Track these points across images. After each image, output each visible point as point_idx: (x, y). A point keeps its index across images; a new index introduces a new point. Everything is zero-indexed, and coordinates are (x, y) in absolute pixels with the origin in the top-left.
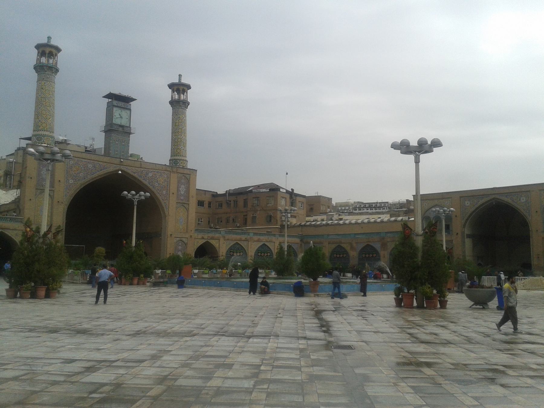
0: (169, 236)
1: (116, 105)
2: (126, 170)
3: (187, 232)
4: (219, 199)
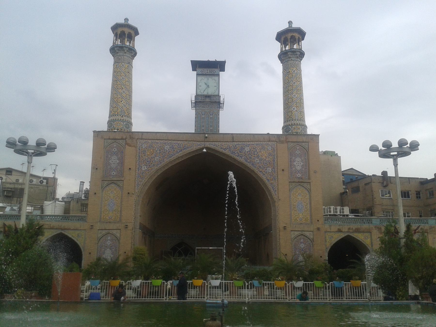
1: (201, 73)
2: (212, 146)
3: (312, 223)
4: (429, 186)
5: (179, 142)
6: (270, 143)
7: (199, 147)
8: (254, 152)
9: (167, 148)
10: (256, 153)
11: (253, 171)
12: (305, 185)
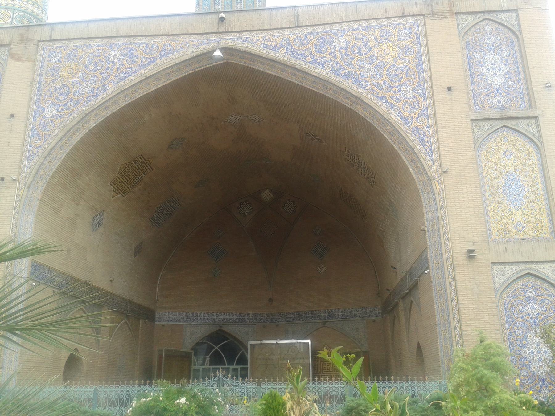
0: (460, 258)
5: (148, 40)
6: (403, 21)
7: (202, 49)
8: (359, 48)
9: (115, 56)
10: (364, 50)
11: (358, 100)
12: (522, 126)
